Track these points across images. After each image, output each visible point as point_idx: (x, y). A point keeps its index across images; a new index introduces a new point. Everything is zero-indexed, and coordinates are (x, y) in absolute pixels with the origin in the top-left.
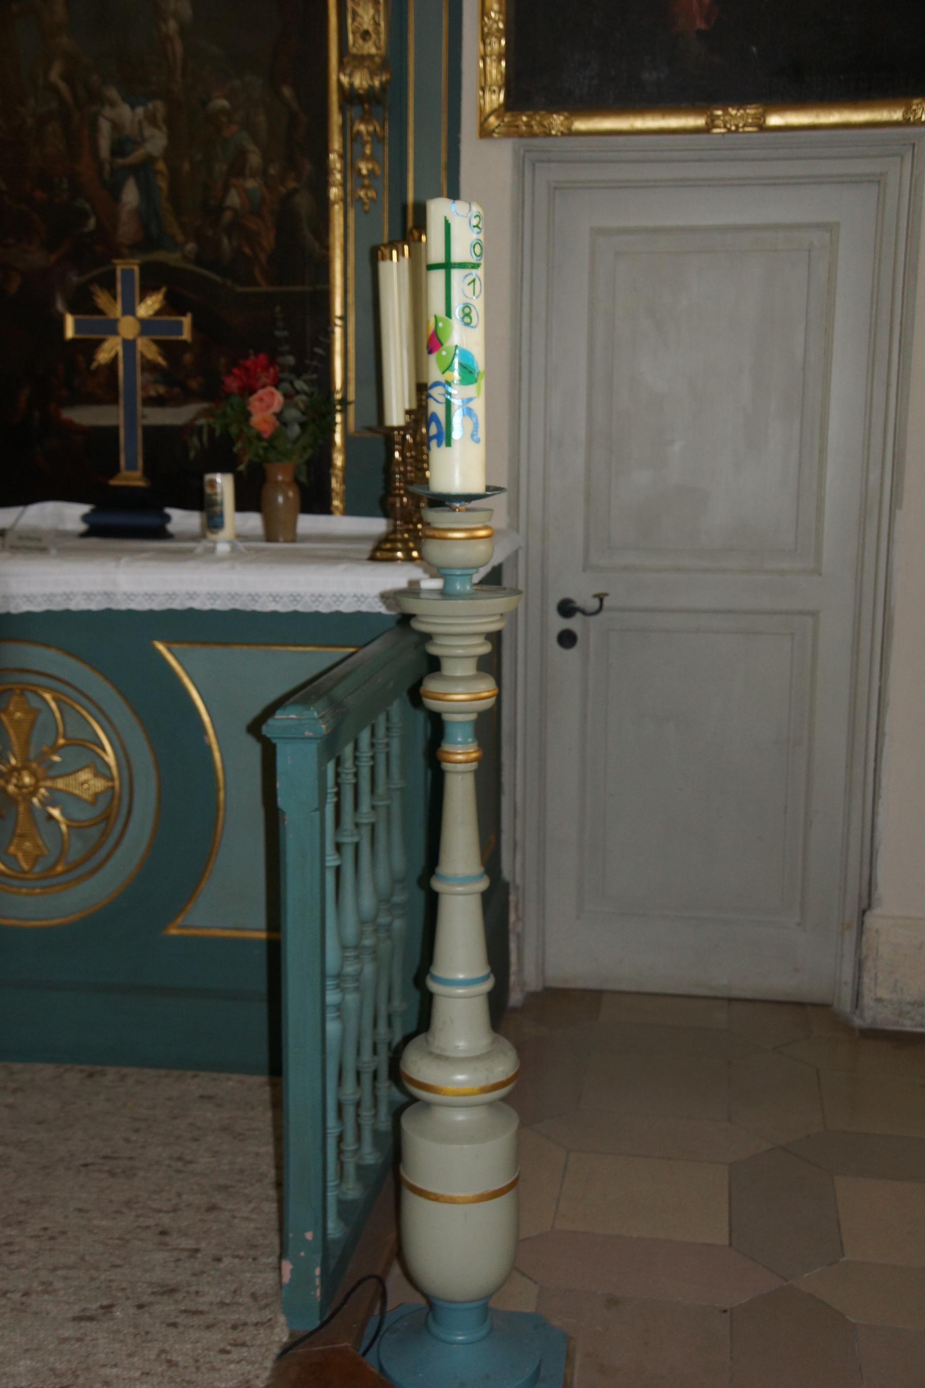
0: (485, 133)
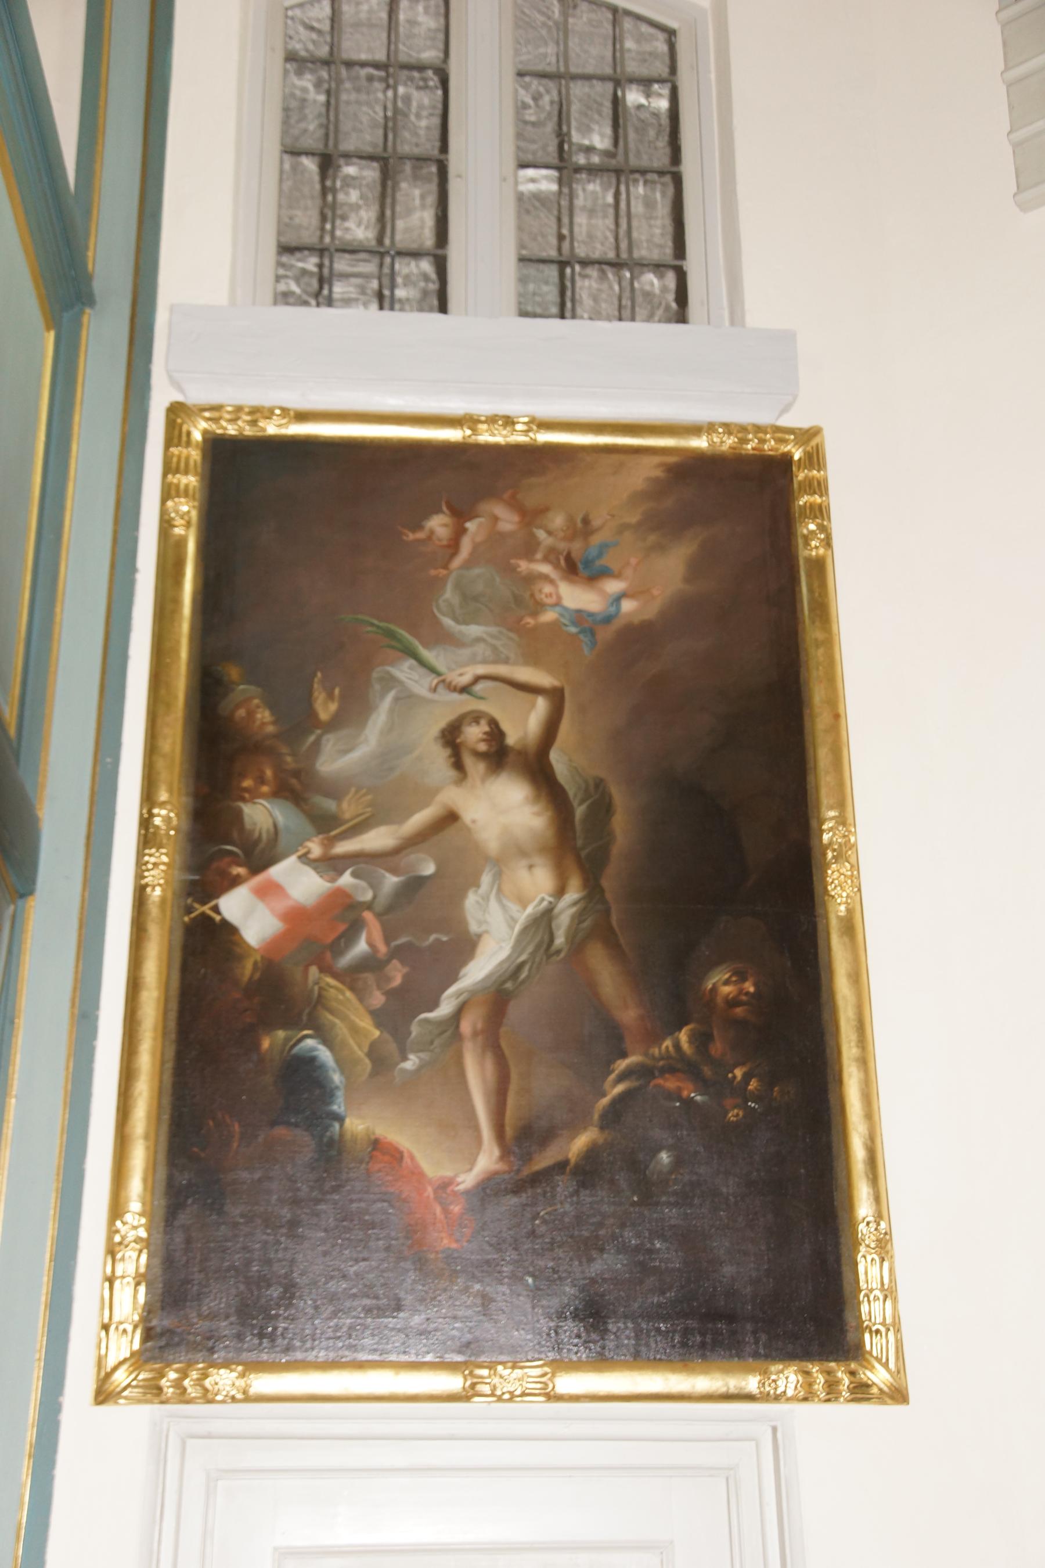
0: (104, 1395)
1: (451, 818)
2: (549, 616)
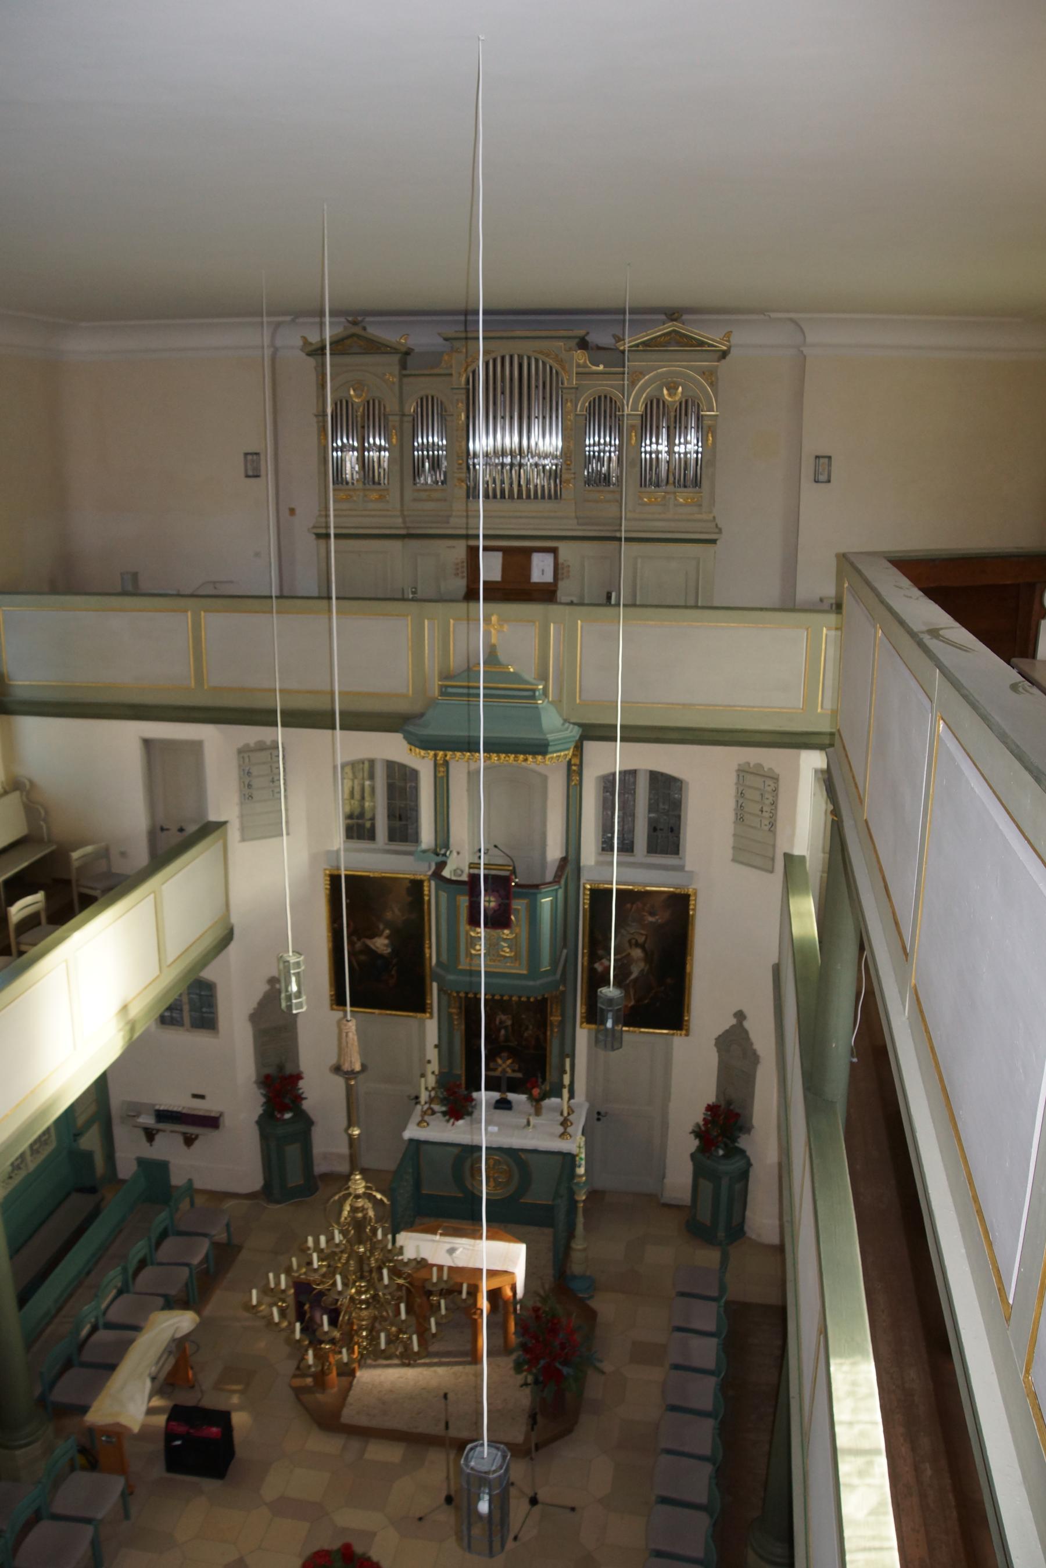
1: (629, 954)
2: (646, 922)
